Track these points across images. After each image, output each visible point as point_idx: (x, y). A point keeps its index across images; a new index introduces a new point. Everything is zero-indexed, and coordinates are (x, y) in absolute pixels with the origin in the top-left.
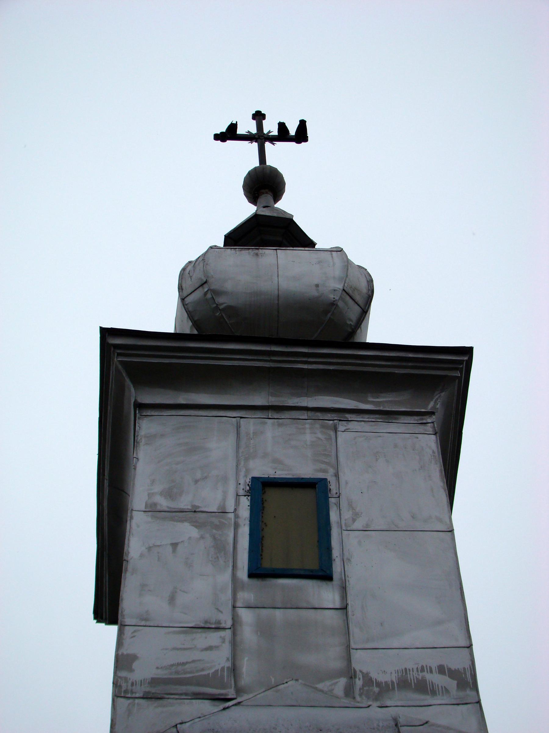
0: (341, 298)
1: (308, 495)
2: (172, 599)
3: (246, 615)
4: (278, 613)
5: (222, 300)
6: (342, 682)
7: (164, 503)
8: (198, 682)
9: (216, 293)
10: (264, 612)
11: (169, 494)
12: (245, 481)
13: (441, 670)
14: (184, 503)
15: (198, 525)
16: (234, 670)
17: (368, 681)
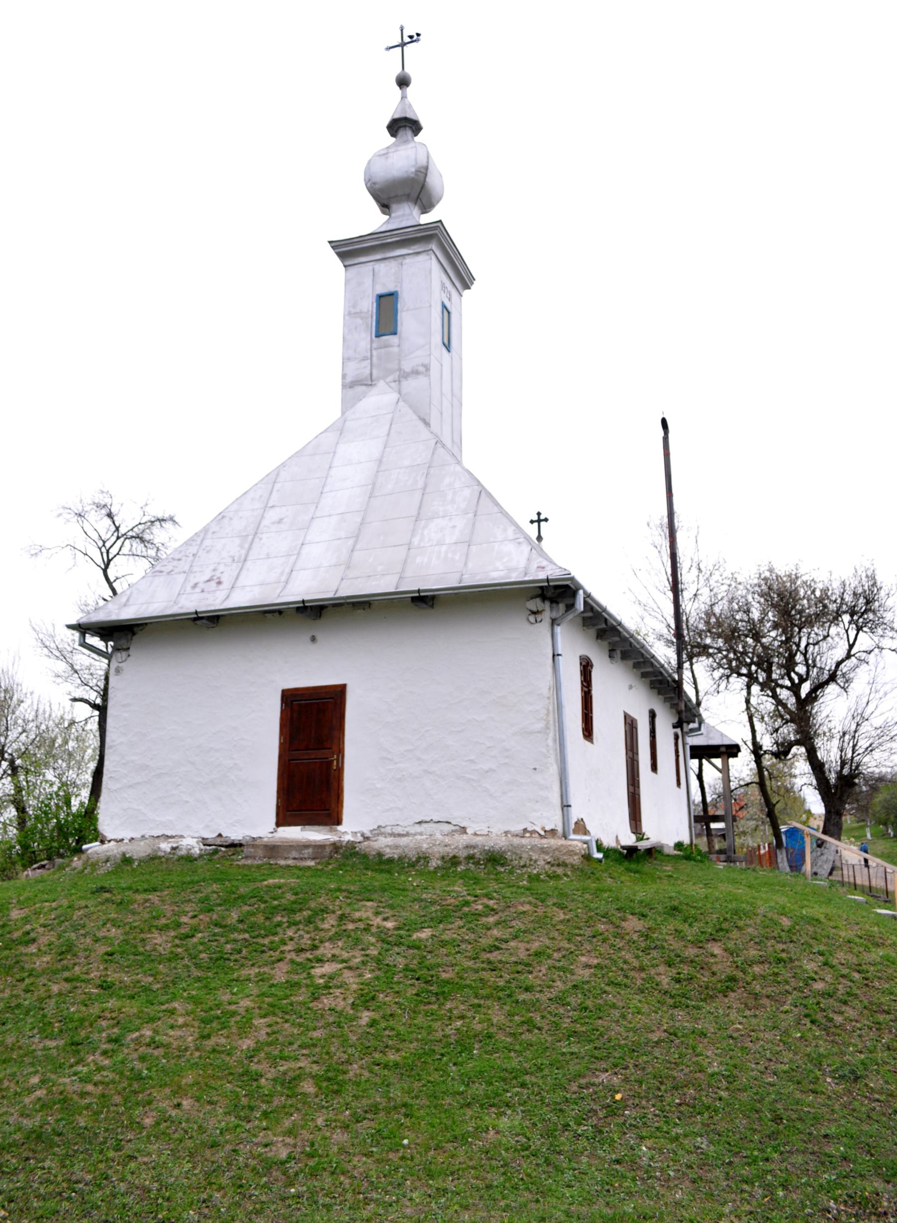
0: (416, 175)
1: (391, 297)
2: (355, 351)
3: (375, 353)
4: (383, 350)
5: (377, 186)
6: (398, 373)
7: (353, 311)
8: (360, 381)
9: (374, 183)
10: (379, 351)
11: (354, 306)
12: (375, 295)
13: (423, 365)
14: (358, 310)
15: (362, 318)
16: (371, 374)
17: (404, 372)
